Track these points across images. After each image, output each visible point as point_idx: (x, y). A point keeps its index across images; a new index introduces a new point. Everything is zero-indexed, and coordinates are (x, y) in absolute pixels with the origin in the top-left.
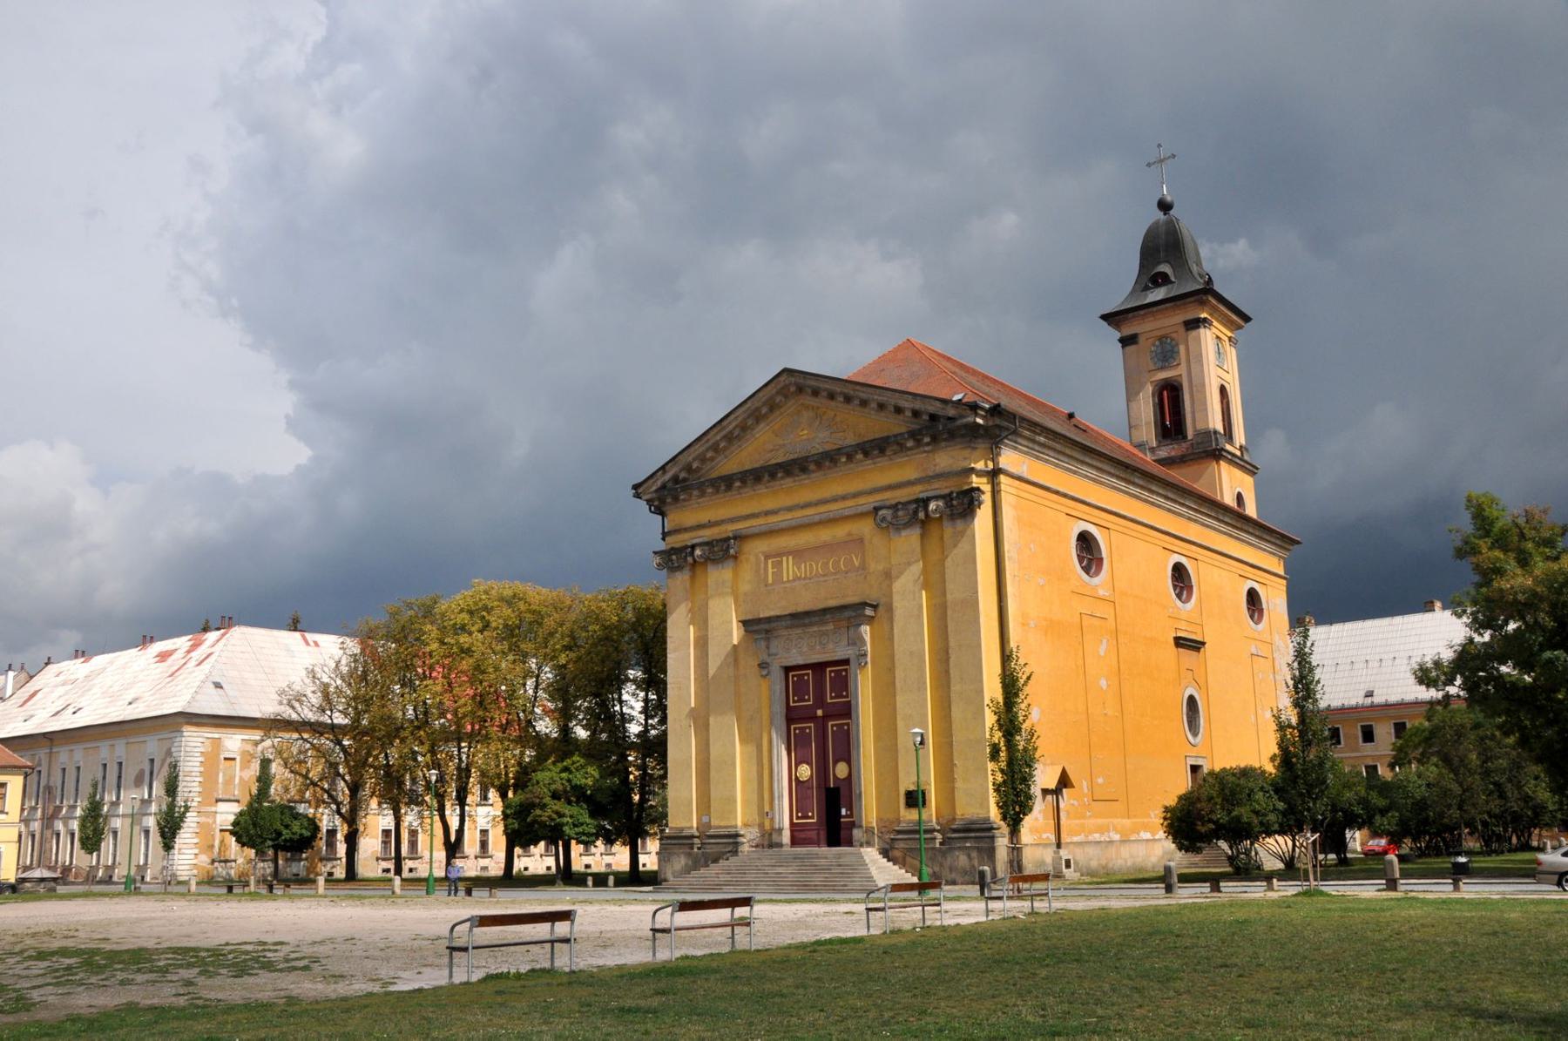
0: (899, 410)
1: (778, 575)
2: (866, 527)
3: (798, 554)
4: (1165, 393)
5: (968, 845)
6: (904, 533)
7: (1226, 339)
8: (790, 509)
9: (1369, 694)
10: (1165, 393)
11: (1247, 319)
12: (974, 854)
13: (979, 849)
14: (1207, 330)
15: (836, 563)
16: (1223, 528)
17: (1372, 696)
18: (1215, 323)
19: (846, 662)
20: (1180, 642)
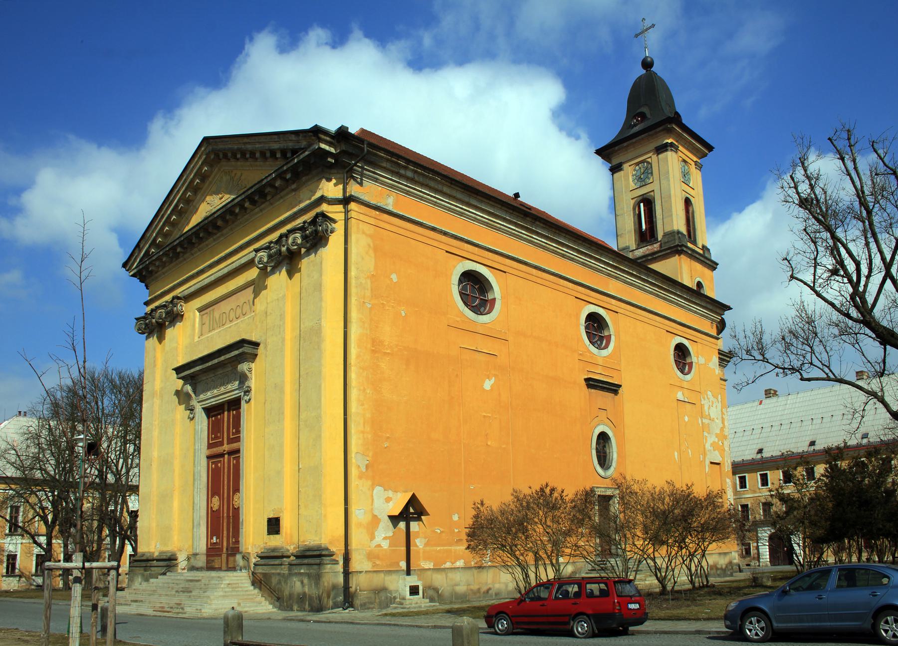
4: (642, 205)
5: (302, 571)
7: (693, 164)
9: (812, 443)
10: (642, 205)
11: (710, 148)
12: (306, 581)
13: (309, 575)
14: (674, 154)
16: (648, 287)
17: (814, 445)
18: (681, 148)
20: (592, 383)
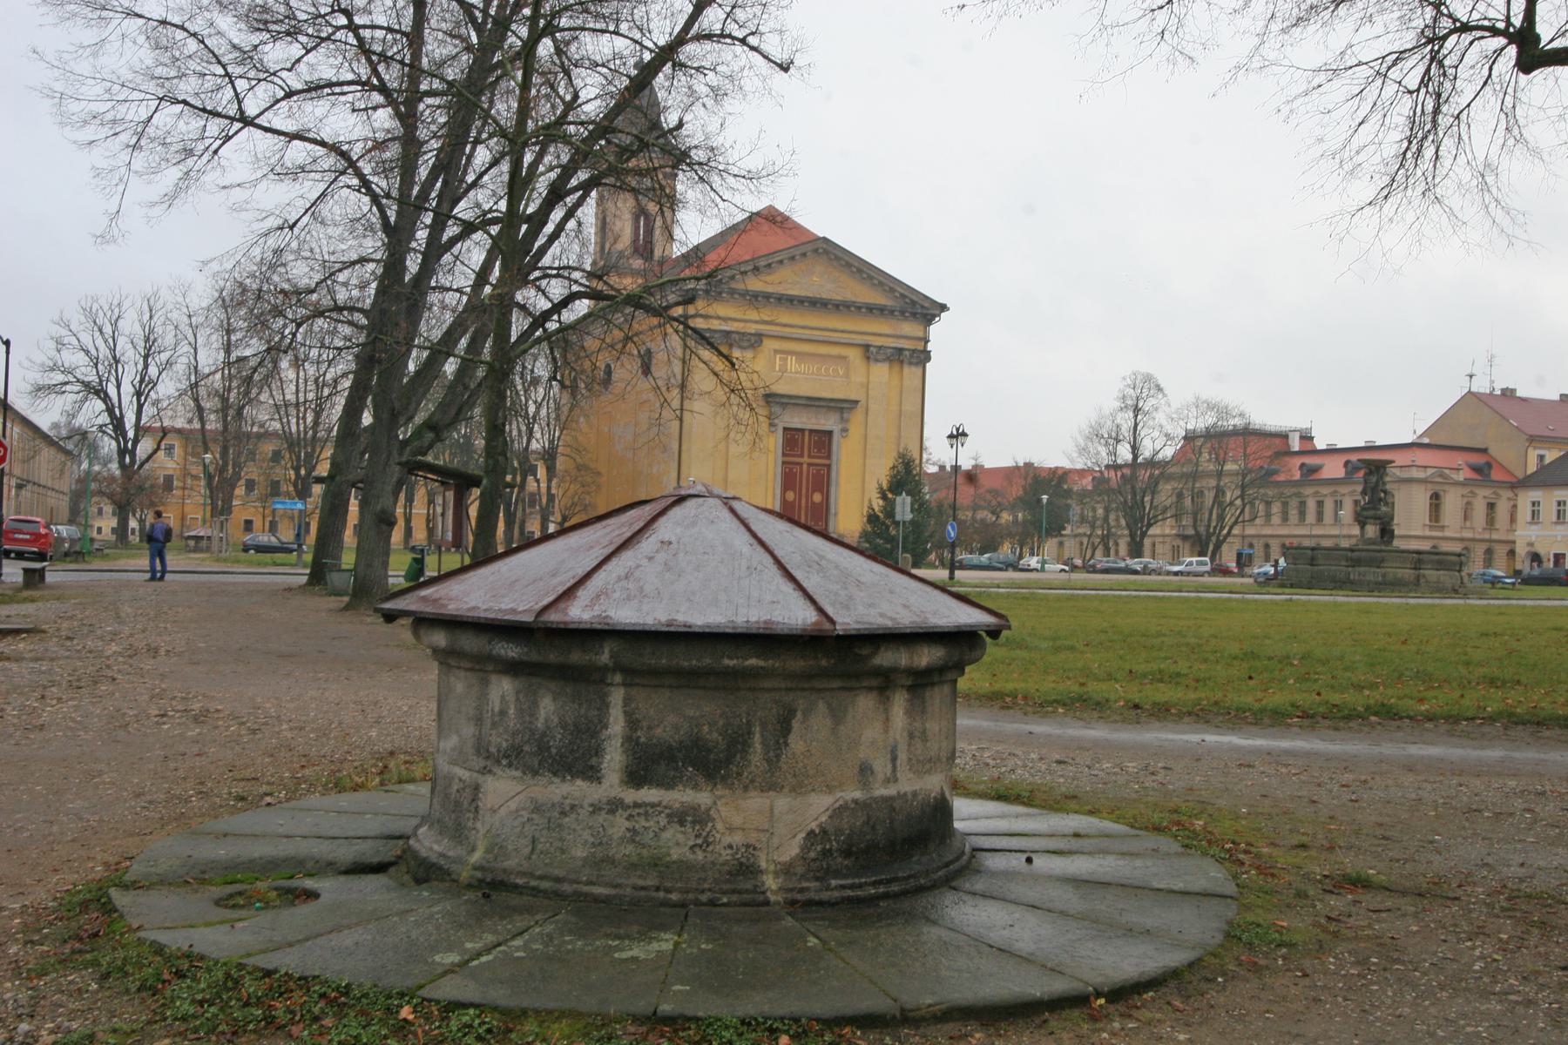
0: (892, 290)
1: (783, 370)
2: (854, 355)
3: (800, 356)
6: (879, 365)
8: (803, 327)
15: (827, 370)
19: (830, 433)
